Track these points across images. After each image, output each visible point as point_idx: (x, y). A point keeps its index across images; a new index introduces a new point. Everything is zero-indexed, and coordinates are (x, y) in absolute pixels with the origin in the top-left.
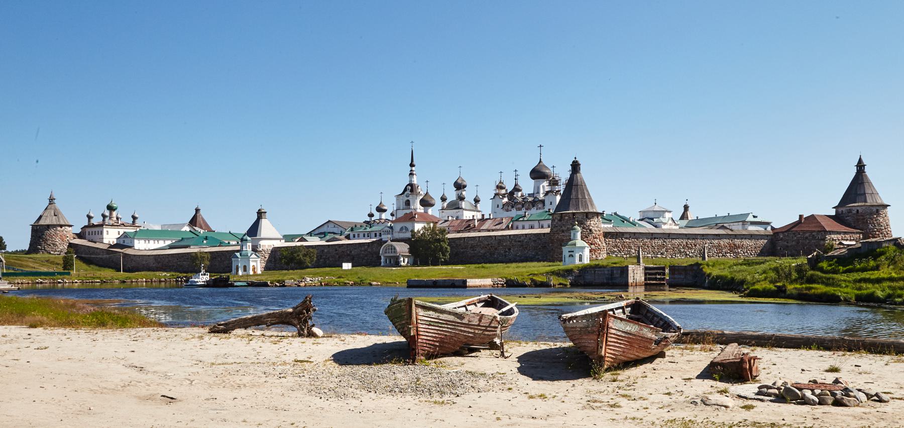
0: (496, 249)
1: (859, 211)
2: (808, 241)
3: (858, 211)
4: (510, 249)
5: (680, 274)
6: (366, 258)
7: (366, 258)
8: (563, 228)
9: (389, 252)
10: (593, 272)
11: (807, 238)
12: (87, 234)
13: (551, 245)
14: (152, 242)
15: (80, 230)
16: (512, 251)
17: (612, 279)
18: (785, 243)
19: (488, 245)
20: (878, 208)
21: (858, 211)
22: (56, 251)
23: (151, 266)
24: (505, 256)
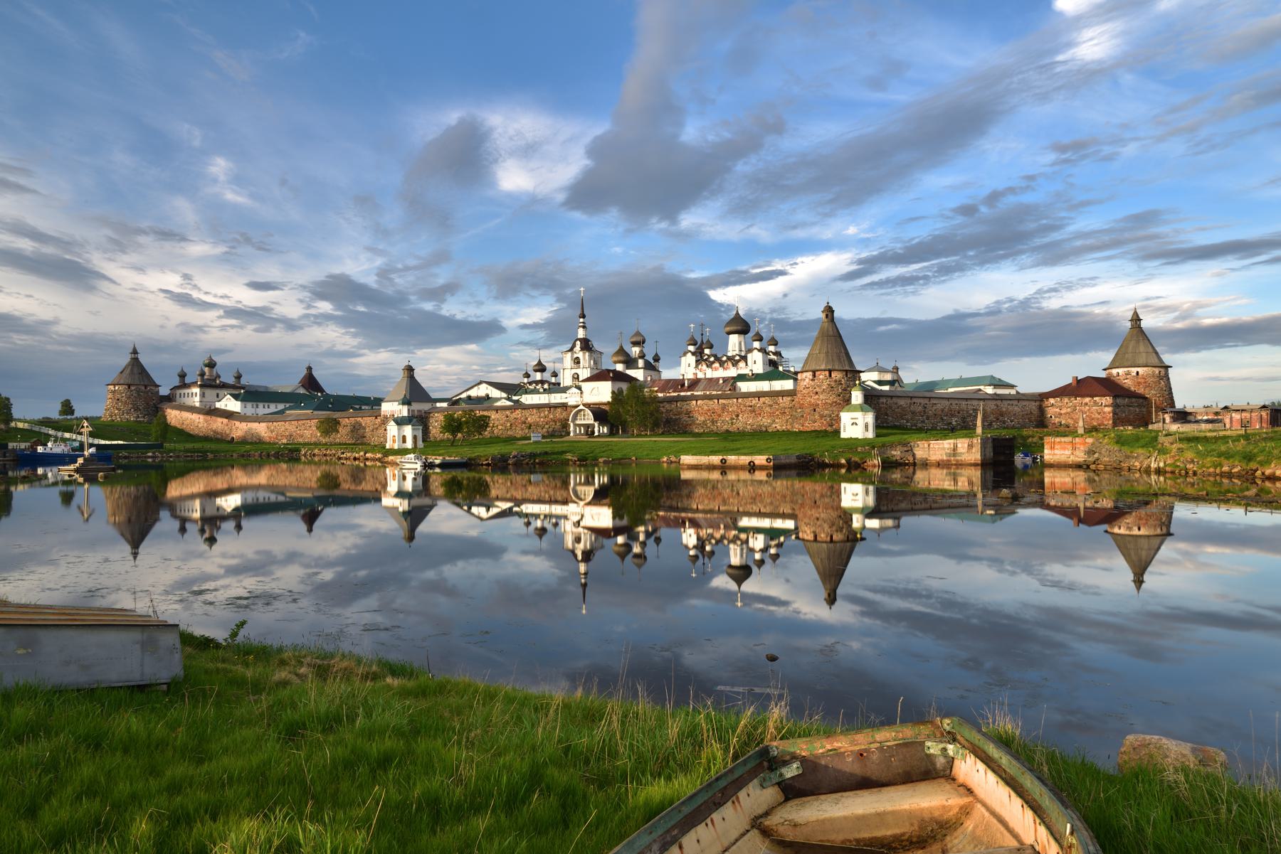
0: (720, 416)
1: (1140, 373)
2: (1087, 408)
3: (1138, 373)
4: (738, 416)
5: (1064, 449)
6: (547, 426)
7: (547, 426)
8: (817, 390)
9: (581, 420)
10: (926, 445)
11: (1086, 404)
12: (178, 396)
13: (799, 410)
14: (261, 405)
15: (169, 392)
16: (740, 418)
17: (954, 455)
18: (1058, 410)
19: (709, 410)
20: (1160, 369)
21: (1138, 373)
22: (138, 417)
23: (263, 434)
24: (732, 423)
